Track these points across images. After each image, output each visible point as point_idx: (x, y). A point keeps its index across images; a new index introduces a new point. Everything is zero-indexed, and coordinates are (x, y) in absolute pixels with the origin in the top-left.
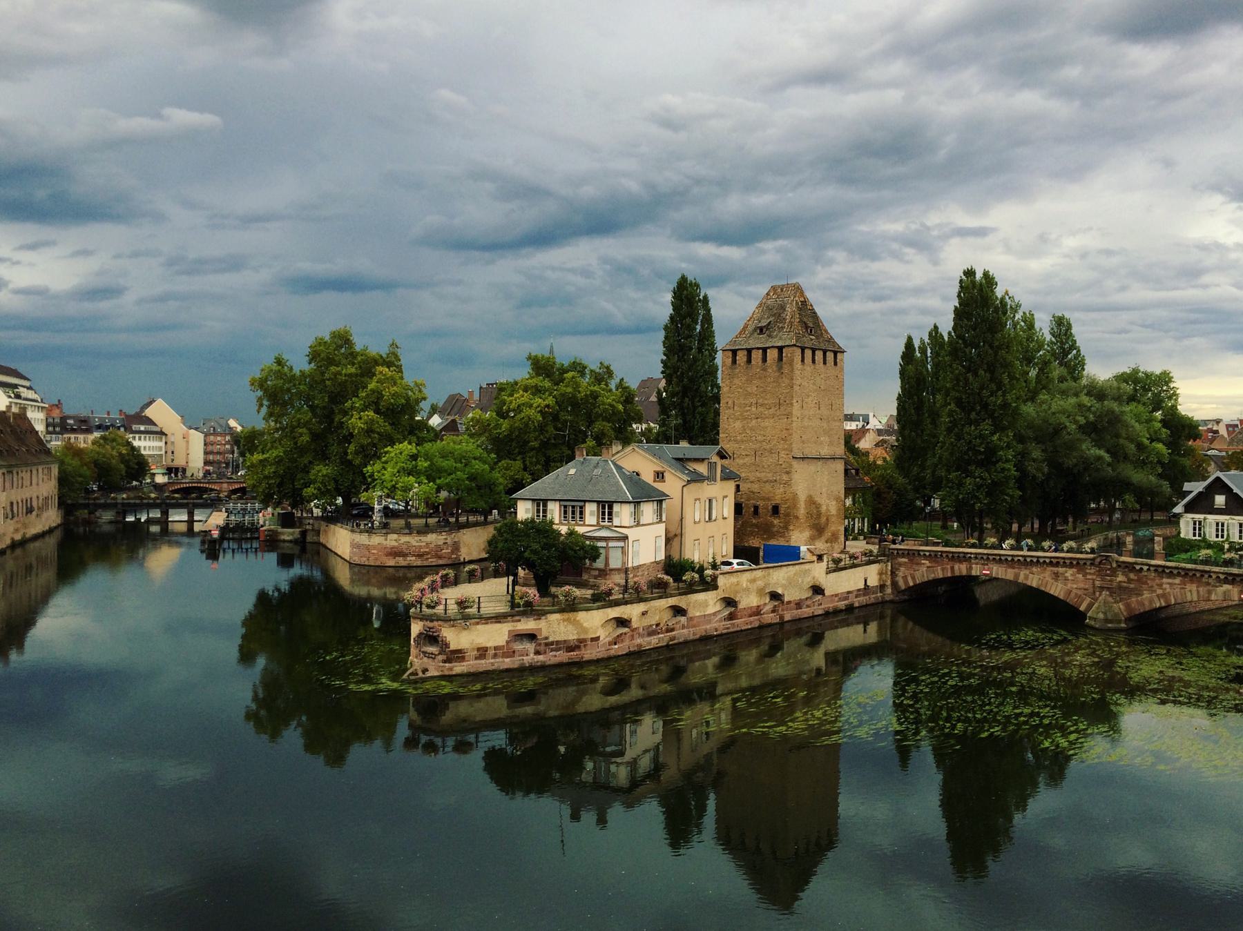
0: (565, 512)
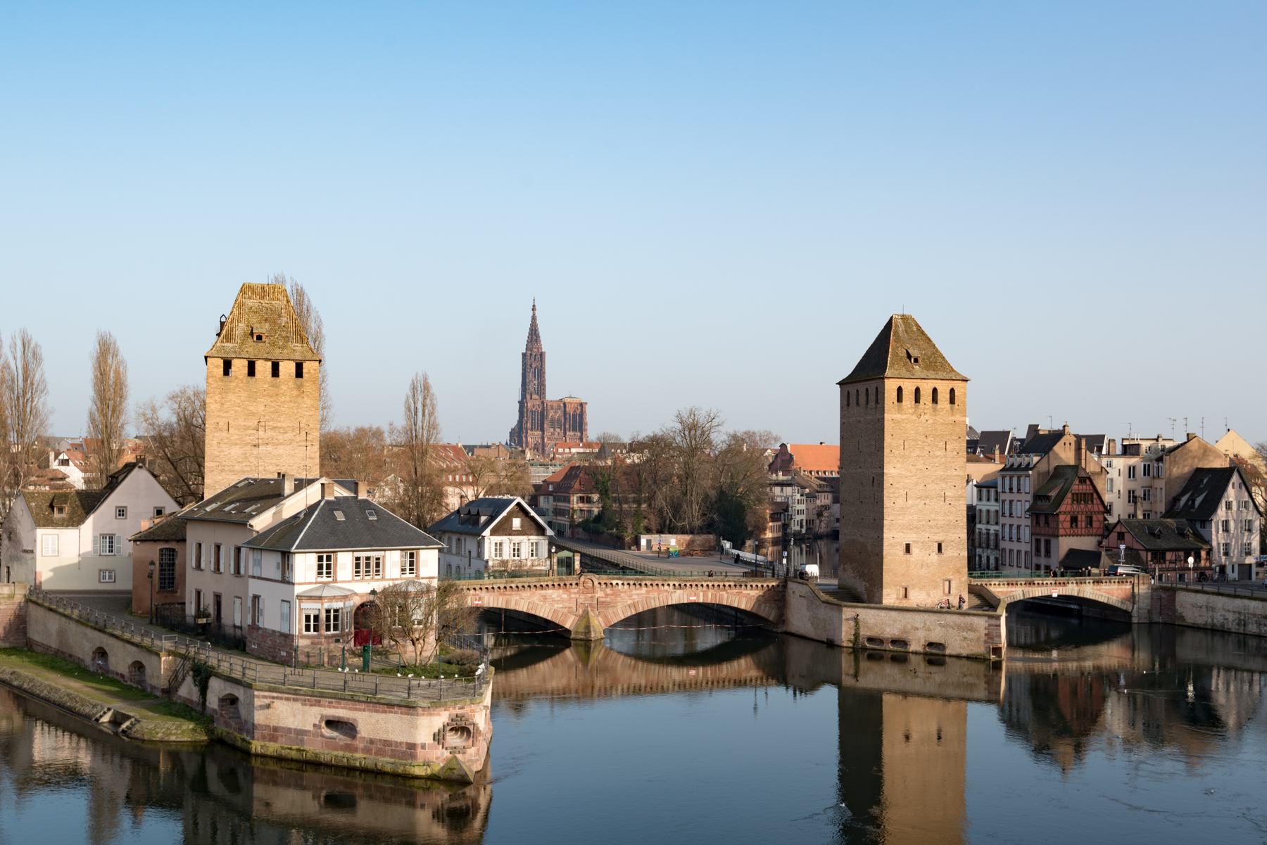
0: (358, 566)
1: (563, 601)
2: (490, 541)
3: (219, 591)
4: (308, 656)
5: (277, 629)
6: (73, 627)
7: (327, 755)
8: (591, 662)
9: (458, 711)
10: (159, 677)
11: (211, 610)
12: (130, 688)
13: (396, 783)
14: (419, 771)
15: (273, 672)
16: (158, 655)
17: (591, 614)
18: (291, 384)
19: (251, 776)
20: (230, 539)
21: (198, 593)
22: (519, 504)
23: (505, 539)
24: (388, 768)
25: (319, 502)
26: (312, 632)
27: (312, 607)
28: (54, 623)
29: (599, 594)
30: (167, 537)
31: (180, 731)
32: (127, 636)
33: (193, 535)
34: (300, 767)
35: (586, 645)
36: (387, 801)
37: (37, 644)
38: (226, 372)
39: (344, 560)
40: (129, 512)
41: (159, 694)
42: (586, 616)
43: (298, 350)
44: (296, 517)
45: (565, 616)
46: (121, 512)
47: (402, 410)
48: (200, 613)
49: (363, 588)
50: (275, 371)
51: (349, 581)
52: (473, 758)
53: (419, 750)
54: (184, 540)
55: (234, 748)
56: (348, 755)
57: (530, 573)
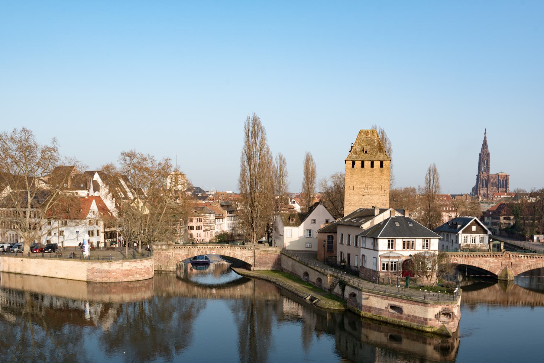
0: (404, 244)
1: (495, 263)
2: (462, 236)
3: (349, 252)
4: (383, 280)
5: (372, 268)
6: (297, 264)
7: (390, 319)
8: (507, 290)
9: (445, 306)
10: (327, 284)
11: (346, 260)
12: (317, 288)
13: (418, 333)
14: (428, 330)
15: (370, 285)
16: (327, 276)
17: (508, 269)
18: (378, 170)
19: (361, 326)
20: (354, 232)
21: (342, 253)
22: (475, 220)
23: (468, 235)
24: (415, 327)
25: (389, 218)
26: (385, 270)
27: (385, 261)
28: (290, 262)
29: (512, 260)
30: (330, 231)
31: (334, 305)
32: (316, 268)
33: (340, 230)
34: (380, 323)
35: (505, 282)
36: (414, 340)
37: (285, 269)
38: (353, 166)
39: (399, 242)
40: (317, 221)
41: (327, 290)
42: (505, 270)
43: (381, 156)
44: (379, 224)
45: (496, 269)
46: (314, 221)
47: (424, 180)
48: (342, 261)
49: (406, 254)
50: (372, 165)
51: (401, 251)
52: (452, 326)
53: (429, 321)
54: (336, 232)
55: (354, 313)
56: (399, 320)
57: (479, 250)
